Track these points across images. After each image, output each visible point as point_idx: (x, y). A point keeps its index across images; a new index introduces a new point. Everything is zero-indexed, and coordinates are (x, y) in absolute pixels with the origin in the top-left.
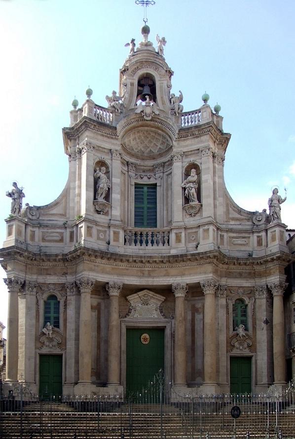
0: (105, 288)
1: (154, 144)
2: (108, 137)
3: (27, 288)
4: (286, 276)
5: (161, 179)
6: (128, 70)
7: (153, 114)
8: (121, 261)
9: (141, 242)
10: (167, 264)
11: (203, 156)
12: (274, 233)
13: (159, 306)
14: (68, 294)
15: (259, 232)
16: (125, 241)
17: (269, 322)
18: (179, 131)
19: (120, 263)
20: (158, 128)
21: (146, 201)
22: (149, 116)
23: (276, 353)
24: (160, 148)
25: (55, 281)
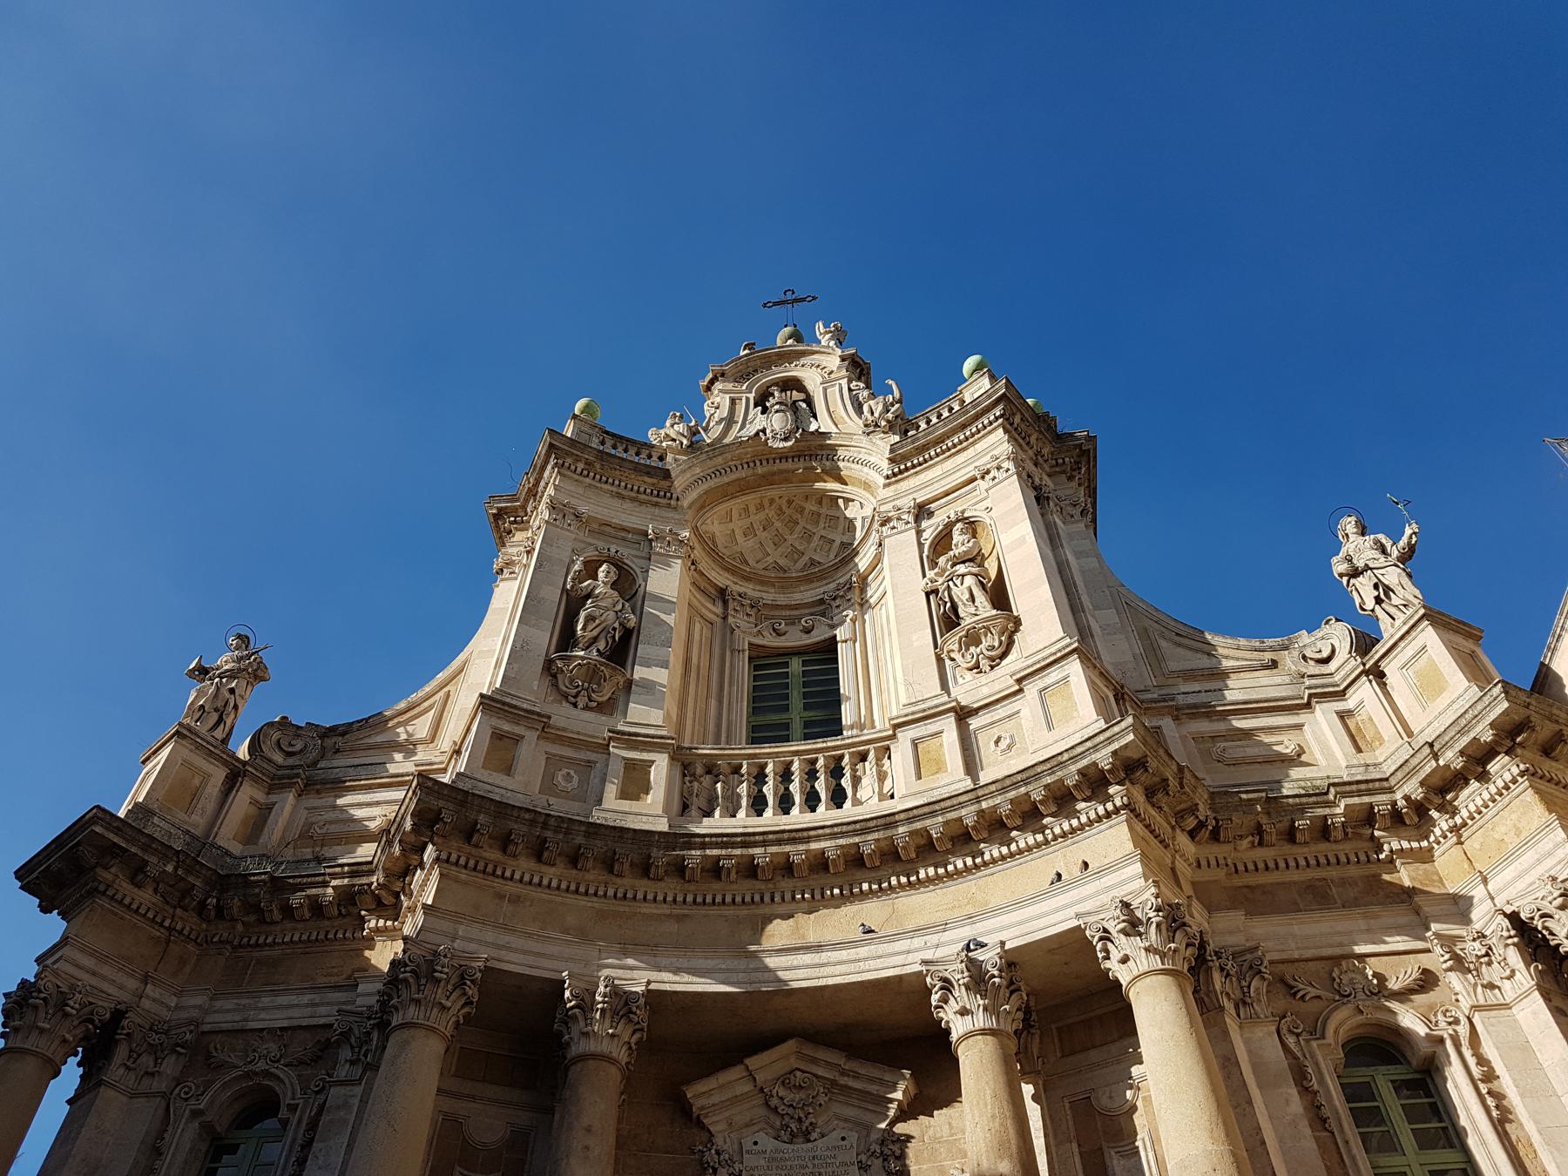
2: (642, 503)
8: (645, 869)
12: (1422, 662)
18: (892, 451)
19: (643, 886)
21: (796, 701)
25: (296, 1013)
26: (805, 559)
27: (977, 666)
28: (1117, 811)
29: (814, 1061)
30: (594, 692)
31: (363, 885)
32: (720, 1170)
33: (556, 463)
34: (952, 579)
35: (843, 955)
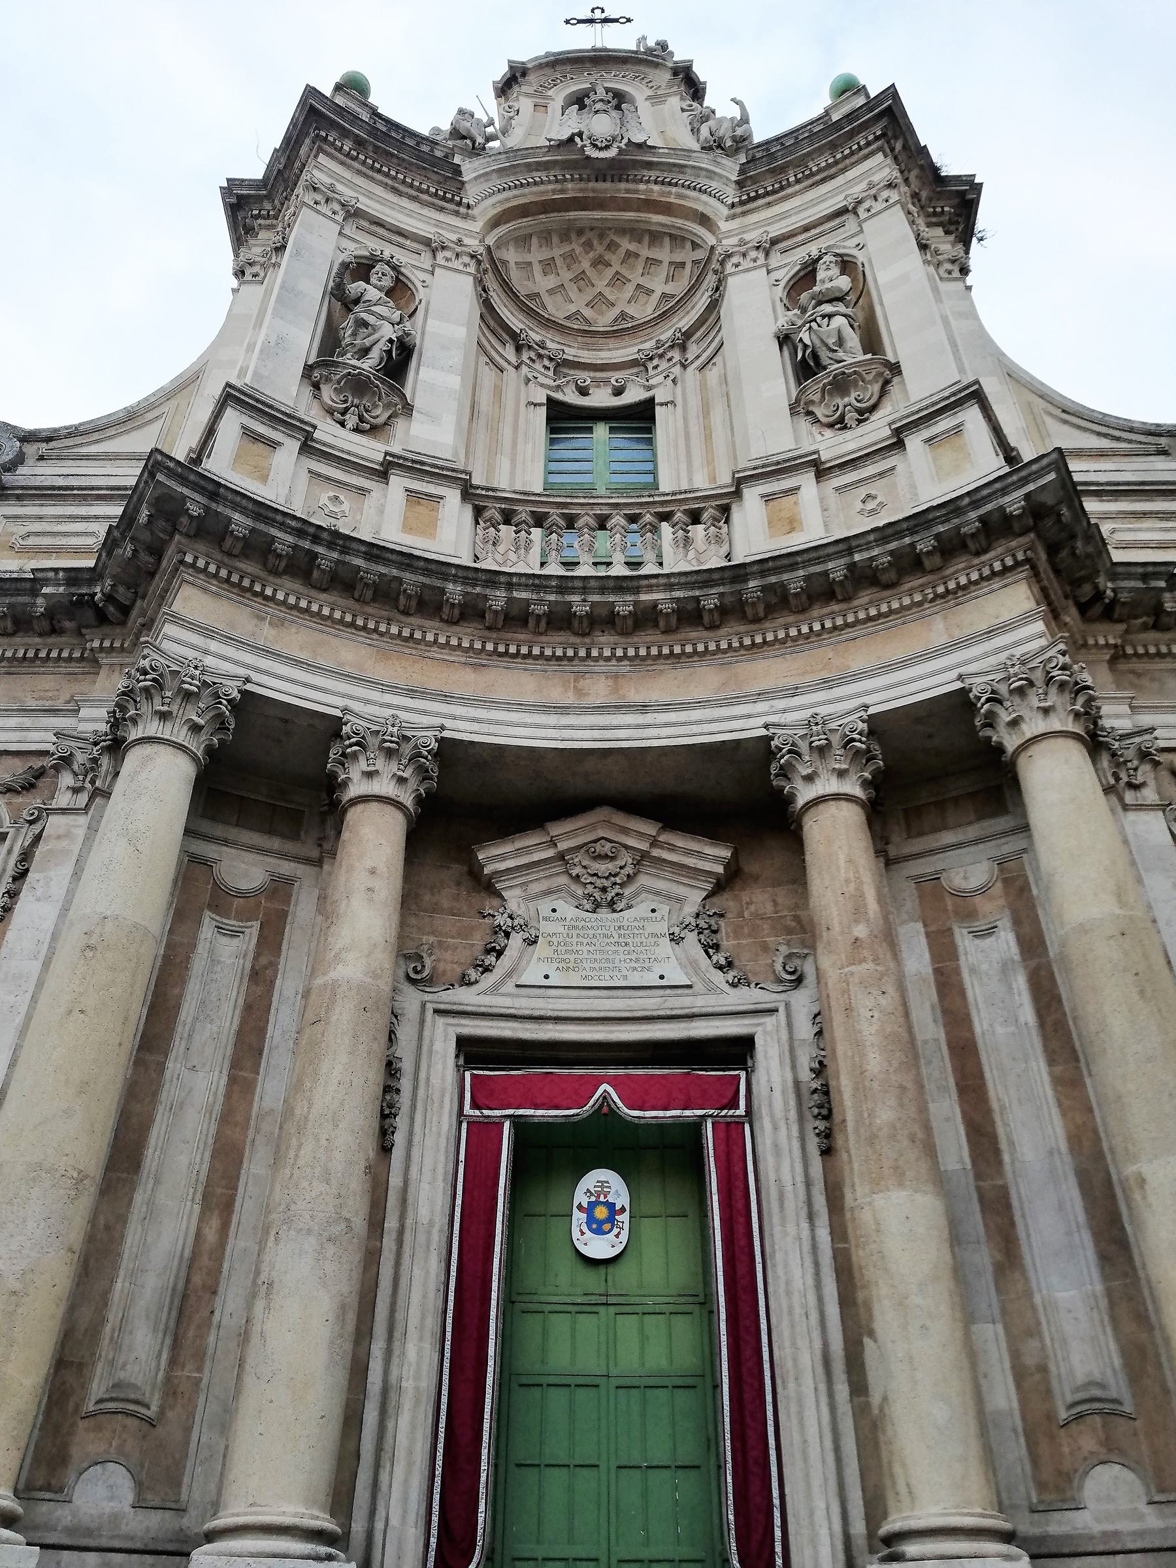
5: (674, 381)
6: (524, 74)
7: (625, 141)
11: (866, 215)
13: (690, 909)
14: (63, 799)
20: (651, 205)
22: (607, 147)
24: (664, 295)
26: (615, 312)
27: (841, 419)
28: (1017, 564)
29: (625, 831)
30: (367, 411)
31: (83, 595)
32: (513, 934)
33: (318, 135)
34: (815, 320)
35: (672, 717)
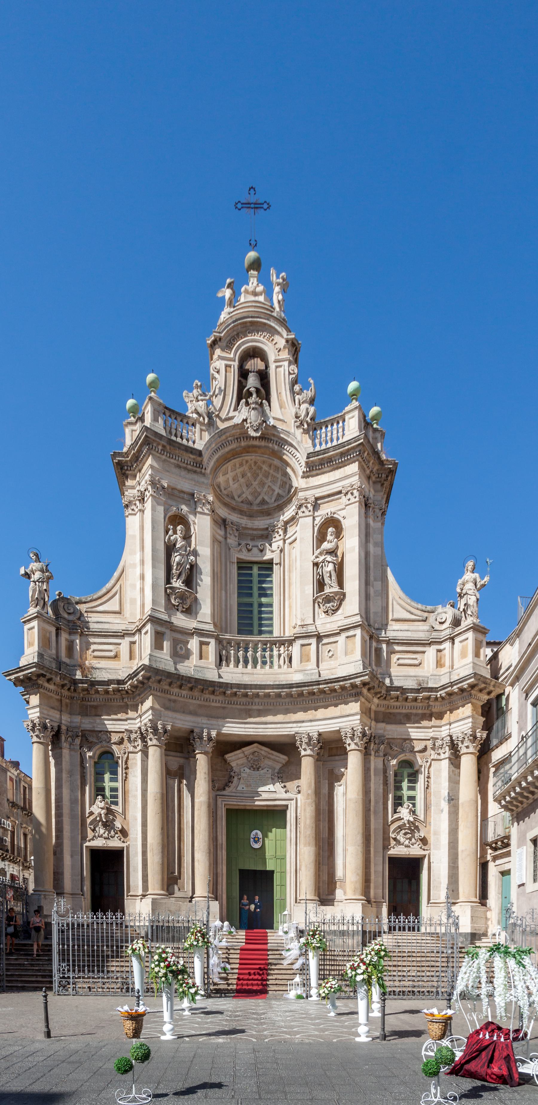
0: (189, 739)
1: (269, 486)
3: (63, 738)
4: (484, 719)
9: (246, 662)
10: (287, 700)
15: (440, 643)
16: (221, 660)
17: (453, 799)
23: (462, 851)
27: (327, 612)
